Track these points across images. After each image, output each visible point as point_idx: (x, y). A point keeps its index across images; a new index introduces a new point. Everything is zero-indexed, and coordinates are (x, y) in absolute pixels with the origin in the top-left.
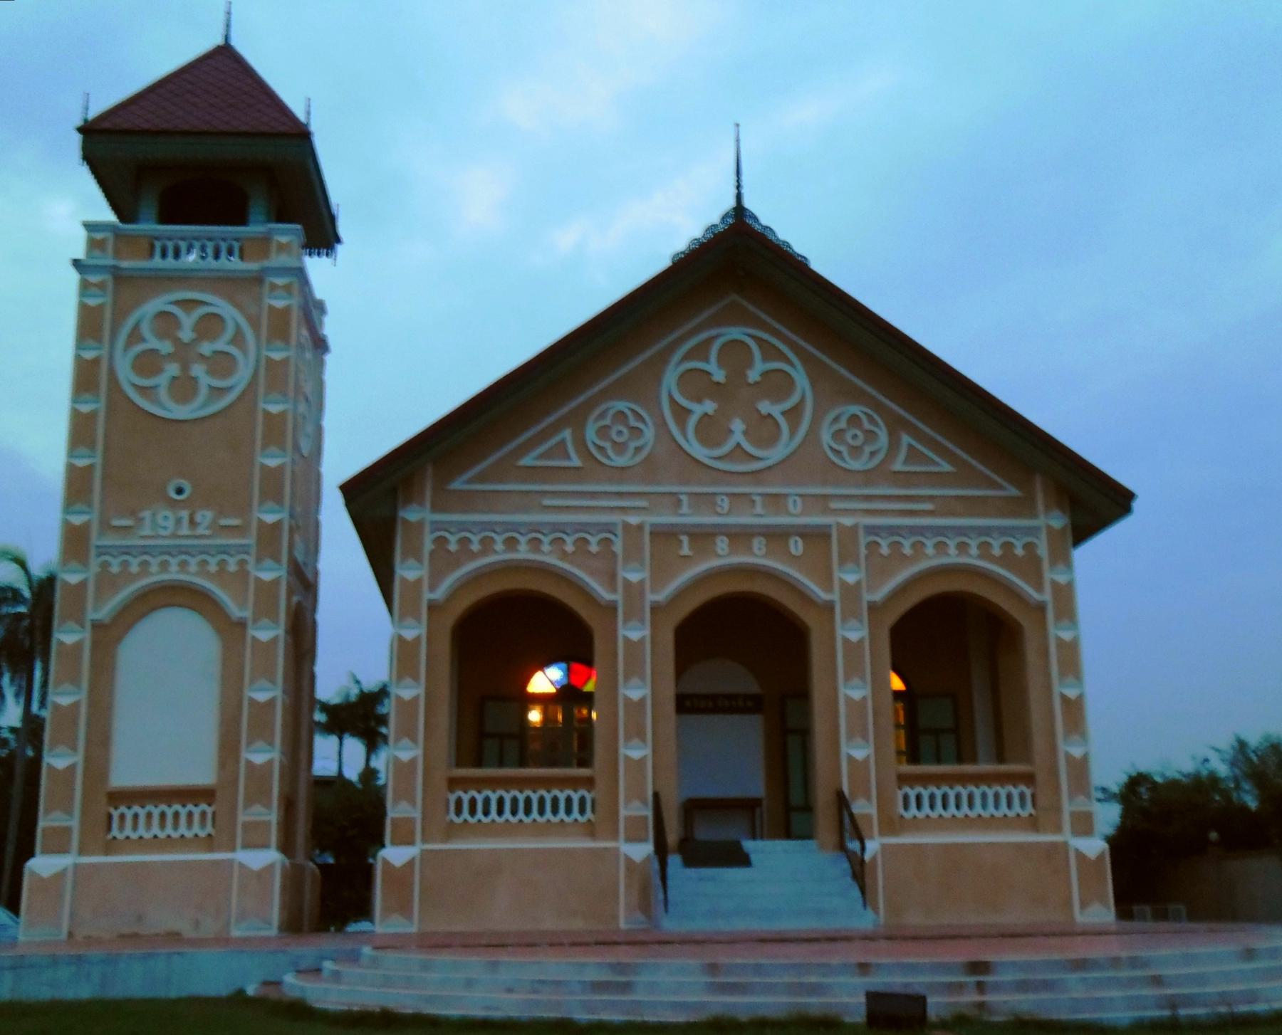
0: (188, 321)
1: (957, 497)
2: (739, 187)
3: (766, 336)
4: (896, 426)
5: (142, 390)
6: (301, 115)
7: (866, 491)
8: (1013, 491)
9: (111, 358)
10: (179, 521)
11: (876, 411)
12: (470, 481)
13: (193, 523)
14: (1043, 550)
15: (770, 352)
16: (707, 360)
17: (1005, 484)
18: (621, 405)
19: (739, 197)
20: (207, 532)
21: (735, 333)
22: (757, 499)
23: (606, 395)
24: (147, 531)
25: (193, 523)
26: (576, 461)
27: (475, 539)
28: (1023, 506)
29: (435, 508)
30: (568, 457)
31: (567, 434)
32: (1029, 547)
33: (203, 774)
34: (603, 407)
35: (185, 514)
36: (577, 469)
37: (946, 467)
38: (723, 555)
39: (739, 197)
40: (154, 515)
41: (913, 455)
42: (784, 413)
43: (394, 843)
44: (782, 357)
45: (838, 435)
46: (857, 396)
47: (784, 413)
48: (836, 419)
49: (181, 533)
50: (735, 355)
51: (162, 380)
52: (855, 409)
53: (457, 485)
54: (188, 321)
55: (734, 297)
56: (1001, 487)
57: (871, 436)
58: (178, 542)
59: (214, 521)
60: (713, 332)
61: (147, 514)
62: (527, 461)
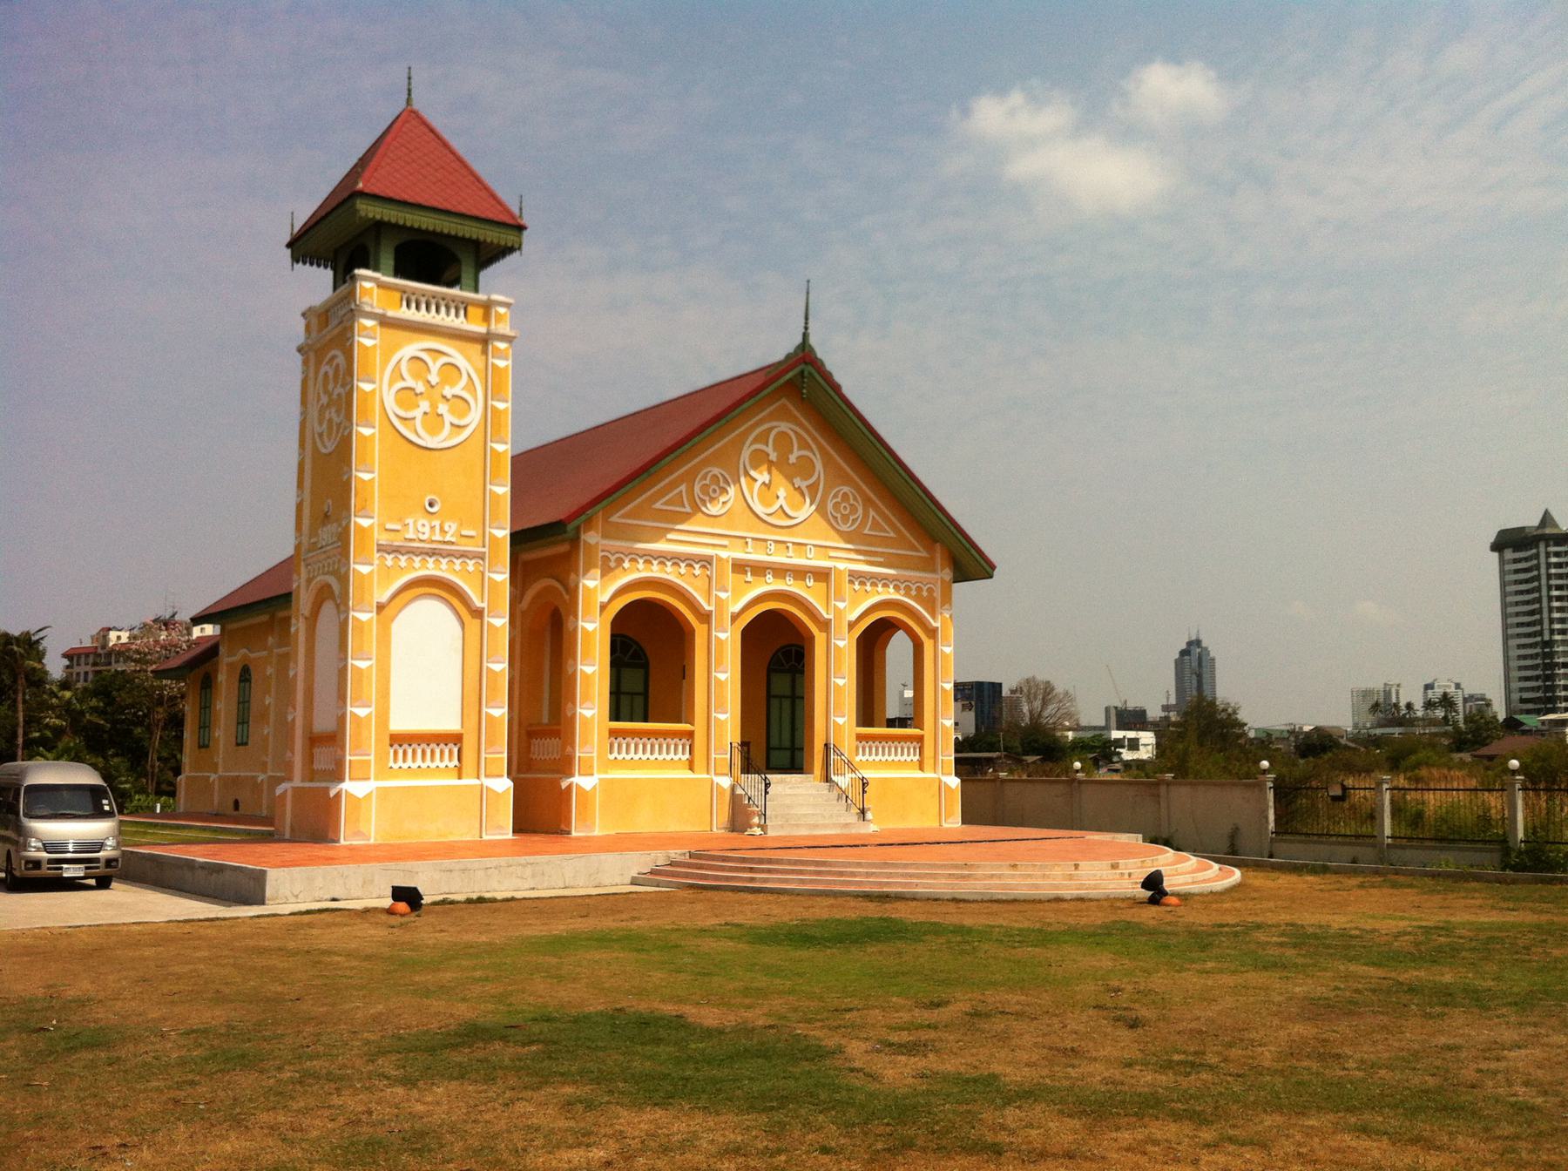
0: (435, 366)
1: (893, 554)
2: (806, 328)
3: (806, 436)
4: (867, 502)
5: (707, 473)
6: (516, 211)
7: (873, 549)
8: (924, 554)
9: (381, 392)
10: (433, 528)
11: (858, 493)
12: (623, 516)
13: (443, 531)
14: (937, 594)
15: (804, 445)
16: (799, 449)
17: (921, 549)
18: (716, 471)
19: (805, 336)
20: (453, 539)
21: (784, 426)
22: (749, 540)
23: (706, 463)
24: (411, 535)
25: (443, 531)
26: (688, 509)
27: (613, 558)
28: (928, 566)
29: (605, 536)
30: (684, 507)
31: (683, 488)
32: (930, 590)
33: (452, 725)
34: (859, 499)
35: (437, 523)
36: (687, 513)
37: (892, 534)
38: (771, 584)
39: (805, 336)
40: (415, 522)
41: (876, 525)
42: (807, 487)
43: (580, 774)
44: (809, 448)
45: (836, 506)
46: (847, 481)
47: (807, 487)
48: (835, 496)
49: (434, 538)
50: (783, 443)
51: (417, 413)
52: (846, 489)
53: (615, 519)
54: (435, 366)
55: (784, 401)
56: (917, 550)
57: (854, 510)
58: (434, 546)
59: (458, 530)
60: (774, 424)
61: (410, 521)
62: (658, 505)
